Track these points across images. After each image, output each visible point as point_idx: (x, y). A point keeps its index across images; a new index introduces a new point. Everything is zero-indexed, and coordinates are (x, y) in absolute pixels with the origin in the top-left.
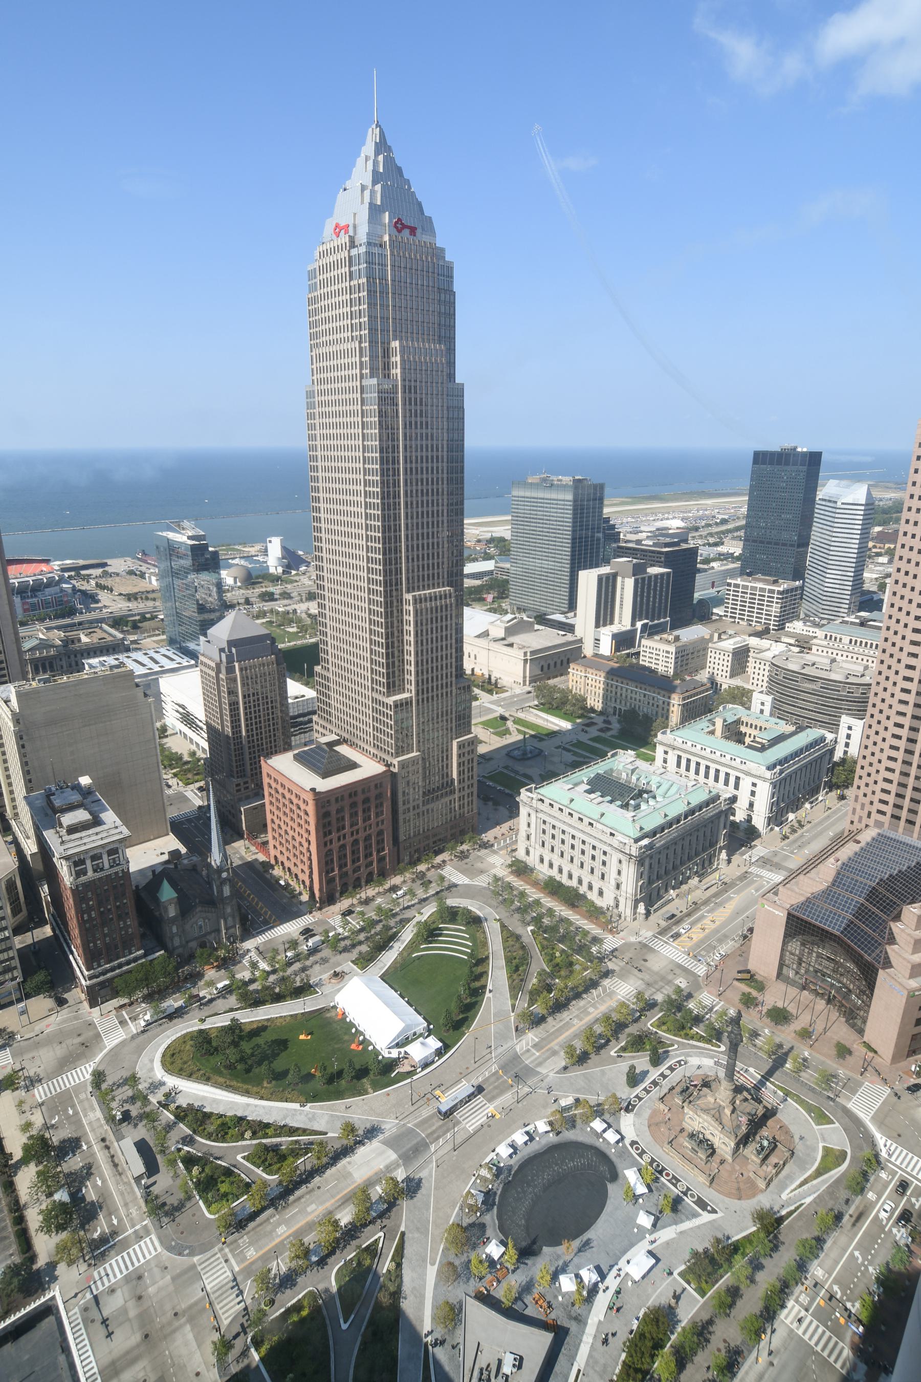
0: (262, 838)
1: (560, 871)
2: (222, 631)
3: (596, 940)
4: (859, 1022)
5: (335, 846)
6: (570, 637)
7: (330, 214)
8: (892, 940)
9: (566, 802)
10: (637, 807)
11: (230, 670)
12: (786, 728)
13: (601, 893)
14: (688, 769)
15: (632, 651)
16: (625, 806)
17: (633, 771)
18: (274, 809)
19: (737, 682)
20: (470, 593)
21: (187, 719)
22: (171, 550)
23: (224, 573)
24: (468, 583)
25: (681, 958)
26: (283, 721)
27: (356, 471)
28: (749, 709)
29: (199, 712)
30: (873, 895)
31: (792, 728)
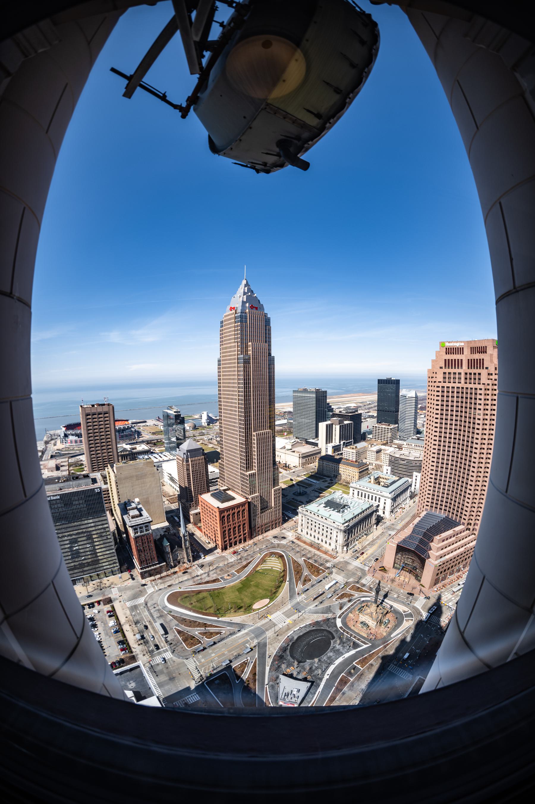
0: (199, 525)
1: (315, 537)
2: (185, 446)
3: (327, 561)
4: (419, 578)
5: (227, 529)
6: (316, 448)
7: (229, 304)
8: (431, 549)
9: (316, 511)
10: (343, 512)
11: (187, 461)
12: (395, 478)
13: (330, 544)
14: (362, 496)
15: (340, 452)
16: (339, 512)
17: (341, 498)
18: (203, 514)
19: (378, 463)
20: (278, 432)
21: (172, 479)
22: (168, 416)
23: (186, 425)
24: (277, 428)
25: (360, 566)
26: (207, 481)
27: (235, 387)
28: (382, 472)
29: (176, 476)
30: (425, 535)
31: (398, 478)
